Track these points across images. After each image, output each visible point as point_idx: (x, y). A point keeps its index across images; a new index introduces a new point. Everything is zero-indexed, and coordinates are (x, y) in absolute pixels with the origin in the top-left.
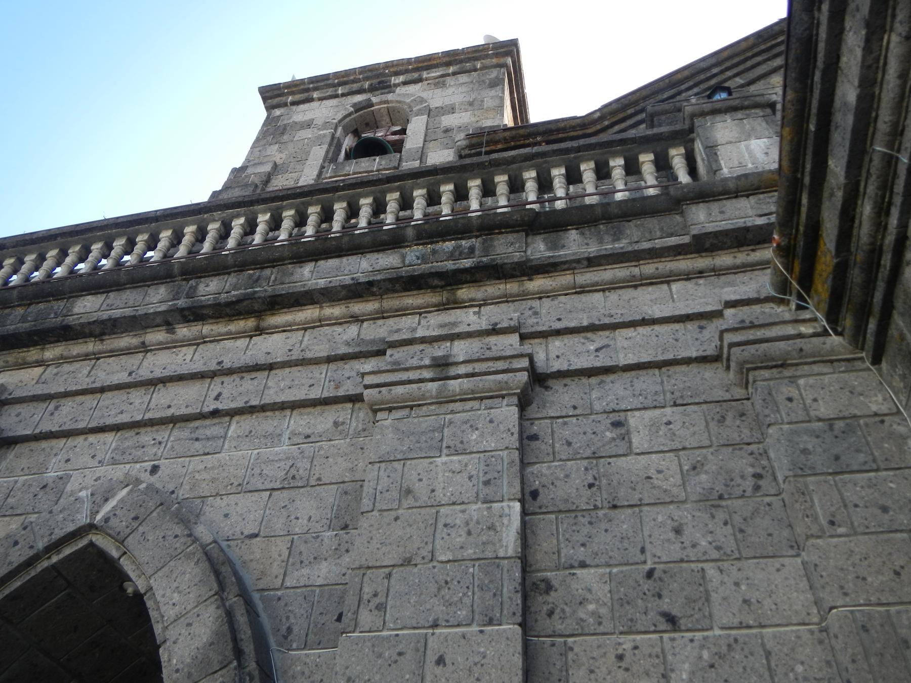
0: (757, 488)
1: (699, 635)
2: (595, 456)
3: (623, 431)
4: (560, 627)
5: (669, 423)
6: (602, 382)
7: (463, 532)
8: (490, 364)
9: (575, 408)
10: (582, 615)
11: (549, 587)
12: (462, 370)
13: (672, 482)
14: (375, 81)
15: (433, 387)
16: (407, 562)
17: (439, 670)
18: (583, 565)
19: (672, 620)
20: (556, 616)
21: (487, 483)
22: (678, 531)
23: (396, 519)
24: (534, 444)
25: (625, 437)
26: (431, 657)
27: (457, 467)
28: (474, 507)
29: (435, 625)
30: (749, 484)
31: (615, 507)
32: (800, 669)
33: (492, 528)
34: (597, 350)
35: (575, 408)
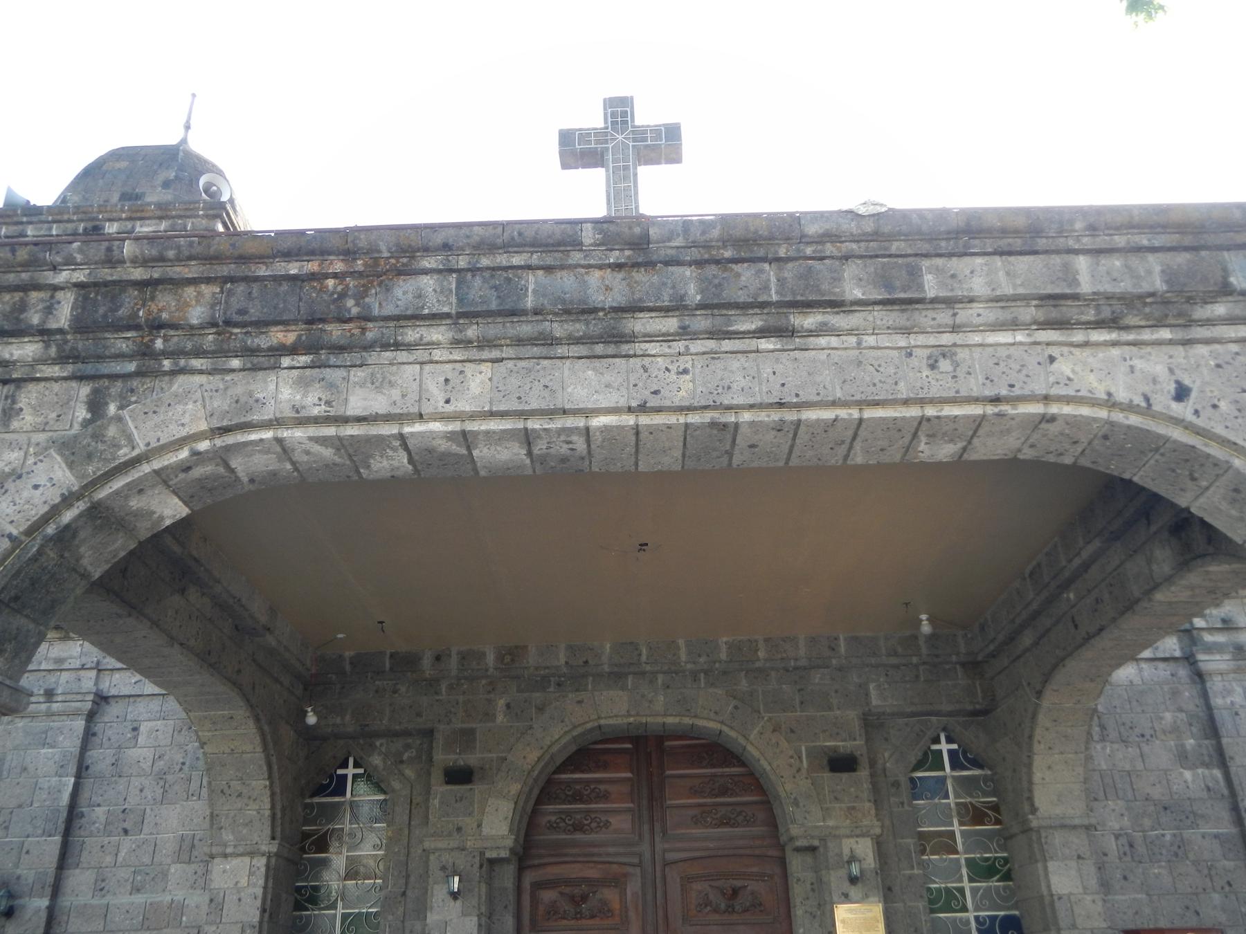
0: (181, 769)
1: (134, 838)
2: (119, 747)
3: (136, 733)
4: (82, 833)
5: (157, 731)
6: (135, 701)
7: (46, 793)
8: (74, 696)
9: (118, 717)
10: (92, 828)
11: (82, 815)
12: (59, 699)
13: (146, 765)
14: (90, 225)
15: (43, 707)
16: (20, 806)
17: (26, 856)
18: (99, 805)
19: (126, 832)
20: (82, 829)
21: (62, 766)
22: (141, 791)
23: (18, 784)
24: (94, 738)
25: (136, 738)
26: (24, 850)
27: (50, 756)
28: (54, 779)
29: (28, 836)
30: (179, 767)
31: (120, 776)
32: (164, 851)
33: (59, 791)
34: (135, 683)
35: (118, 717)
